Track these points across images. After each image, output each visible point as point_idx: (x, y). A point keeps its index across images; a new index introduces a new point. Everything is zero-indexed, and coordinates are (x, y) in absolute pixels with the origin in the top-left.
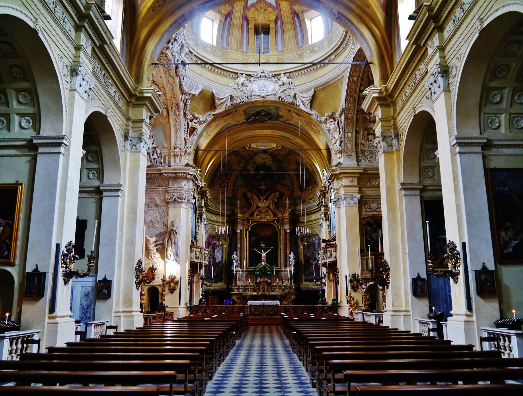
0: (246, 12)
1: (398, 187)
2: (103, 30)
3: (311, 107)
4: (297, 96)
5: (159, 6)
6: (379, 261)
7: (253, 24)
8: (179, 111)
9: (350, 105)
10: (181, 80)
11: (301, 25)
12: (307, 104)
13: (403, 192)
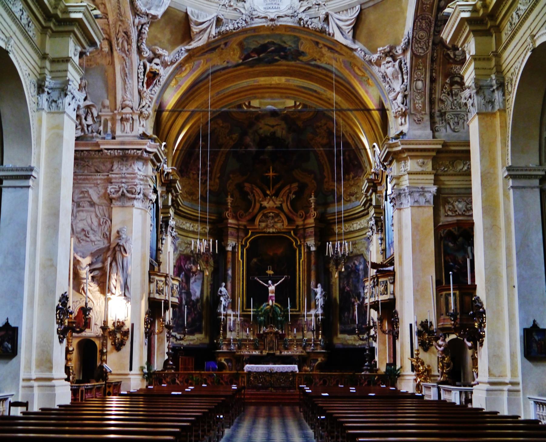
1: (501, 173)
3: (354, 37)
4: (330, 18)
6: (467, 299)
8: (129, 44)
9: (422, 33)
12: (347, 31)
13: (511, 183)
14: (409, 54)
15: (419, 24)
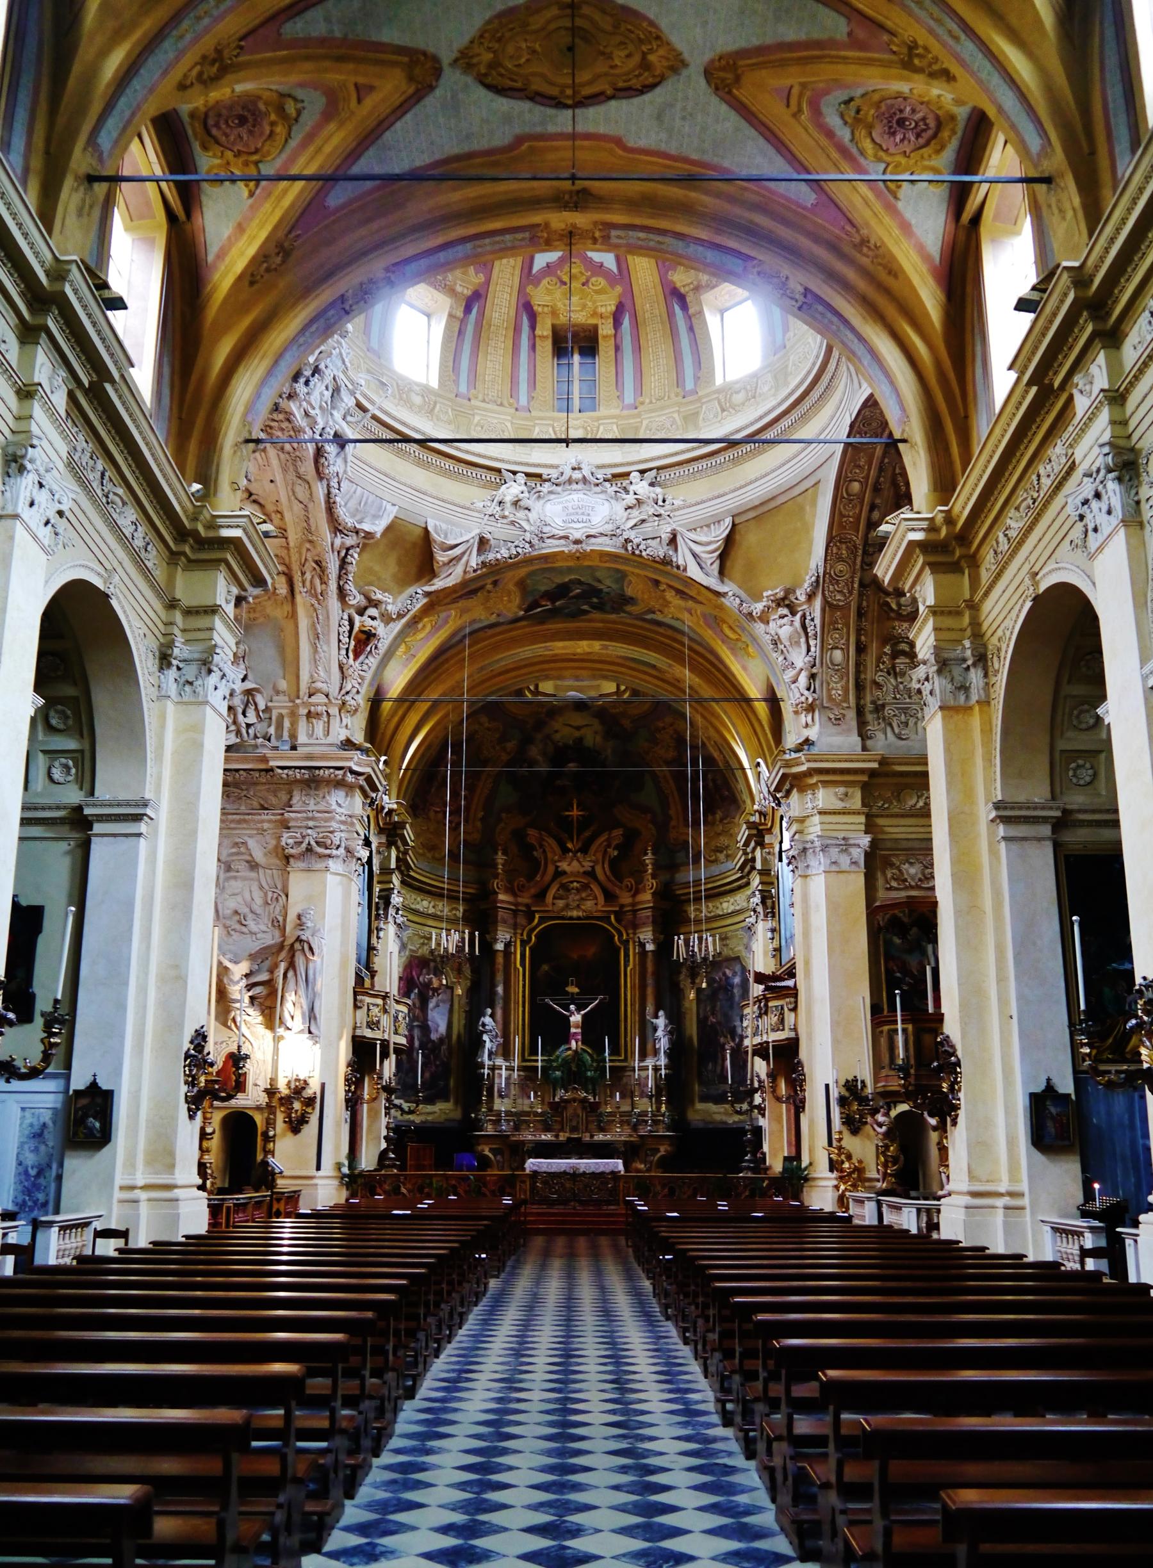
0: (529, 289)
1: (985, 813)
2: (103, 340)
3: (722, 572)
4: (679, 538)
5: (268, 270)
6: (927, 1038)
7: (549, 326)
8: (324, 582)
9: (840, 567)
10: (332, 490)
11: (691, 329)
12: (709, 562)
13: (1001, 830)
14: (818, 603)
15: (835, 550)
